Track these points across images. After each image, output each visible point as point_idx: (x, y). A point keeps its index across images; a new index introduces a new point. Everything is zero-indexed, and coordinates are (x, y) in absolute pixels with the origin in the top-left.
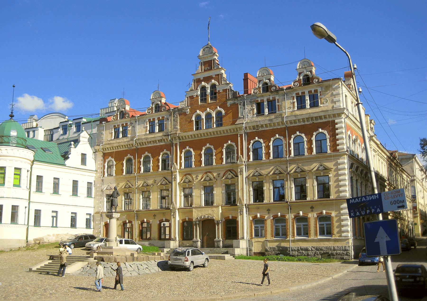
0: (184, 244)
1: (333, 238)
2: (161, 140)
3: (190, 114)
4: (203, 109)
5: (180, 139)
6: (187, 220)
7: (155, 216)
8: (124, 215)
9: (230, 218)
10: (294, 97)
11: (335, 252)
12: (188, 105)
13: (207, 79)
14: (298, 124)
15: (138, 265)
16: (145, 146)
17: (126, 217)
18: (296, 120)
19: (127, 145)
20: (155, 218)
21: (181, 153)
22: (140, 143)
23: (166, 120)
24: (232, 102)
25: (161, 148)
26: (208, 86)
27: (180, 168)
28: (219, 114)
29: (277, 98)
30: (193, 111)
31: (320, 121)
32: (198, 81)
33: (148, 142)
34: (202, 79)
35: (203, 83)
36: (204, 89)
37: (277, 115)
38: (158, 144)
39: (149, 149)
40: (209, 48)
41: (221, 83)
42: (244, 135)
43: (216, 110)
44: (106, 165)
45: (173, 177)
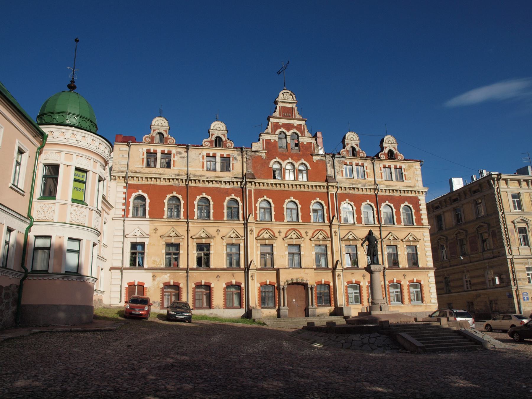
0: (263, 313)
3: (267, 159)
6: (268, 283)
7: (220, 277)
8: (166, 274)
9: (323, 282)
10: (381, 168)
12: (264, 149)
13: (288, 127)
14: (387, 194)
16: (201, 185)
17: (169, 277)
18: (386, 190)
19: (173, 179)
20: (218, 280)
21: (256, 201)
22: (195, 180)
23: (233, 160)
24: (318, 158)
25: (228, 192)
26: (289, 133)
29: (365, 164)
30: (270, 157)
31: (406, 195)
32: (277, 126)
33: (208, 181)
34: (281, 124)
37: (366, 181)
38: (223, 186)
39: (208, 190)
40: (289, 94)
41: (305, 135)
43: (301, 162)
44: (131, 200)
45: (249, 230)
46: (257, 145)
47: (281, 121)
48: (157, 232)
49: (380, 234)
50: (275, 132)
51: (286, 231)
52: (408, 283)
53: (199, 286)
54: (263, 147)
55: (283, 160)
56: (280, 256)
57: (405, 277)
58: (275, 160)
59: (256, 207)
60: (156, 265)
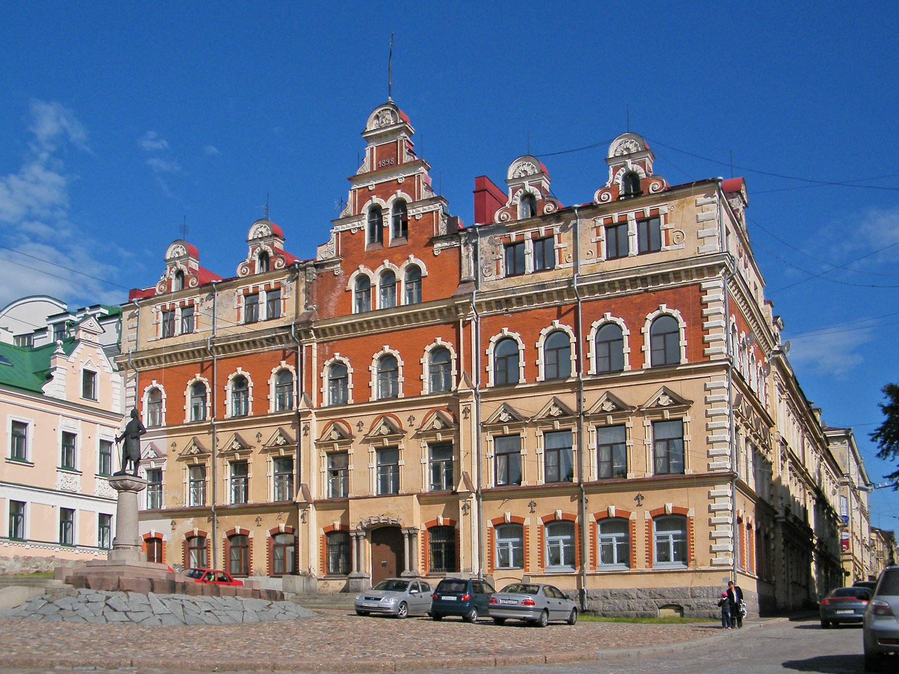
1: (690, 569)
2: (273, 338)
4: (373, 261)
5: (317, 335)
11: (693, 602)
12: (337, 255)
15: (185, 603)
26: (388, 205)
27: (319, 407)
28: (413, 271)
35: (376, 200)
36: (376, 211)
41: (419, 197)
42: (473, 323)
45: (302, 426)
46: (326, 250)
47: (372, 184)
48: (176, 448)
49: (579, 401)
50: (360, 210)
51: (371, 419)
52: (648, 516)
53: (232, 536)
54: (338, 251)
55: (373, 269)
56: (360, 473)
57: (642, 502)
58: (356, 273)
59: (320, 379)
60: (177, 504)
